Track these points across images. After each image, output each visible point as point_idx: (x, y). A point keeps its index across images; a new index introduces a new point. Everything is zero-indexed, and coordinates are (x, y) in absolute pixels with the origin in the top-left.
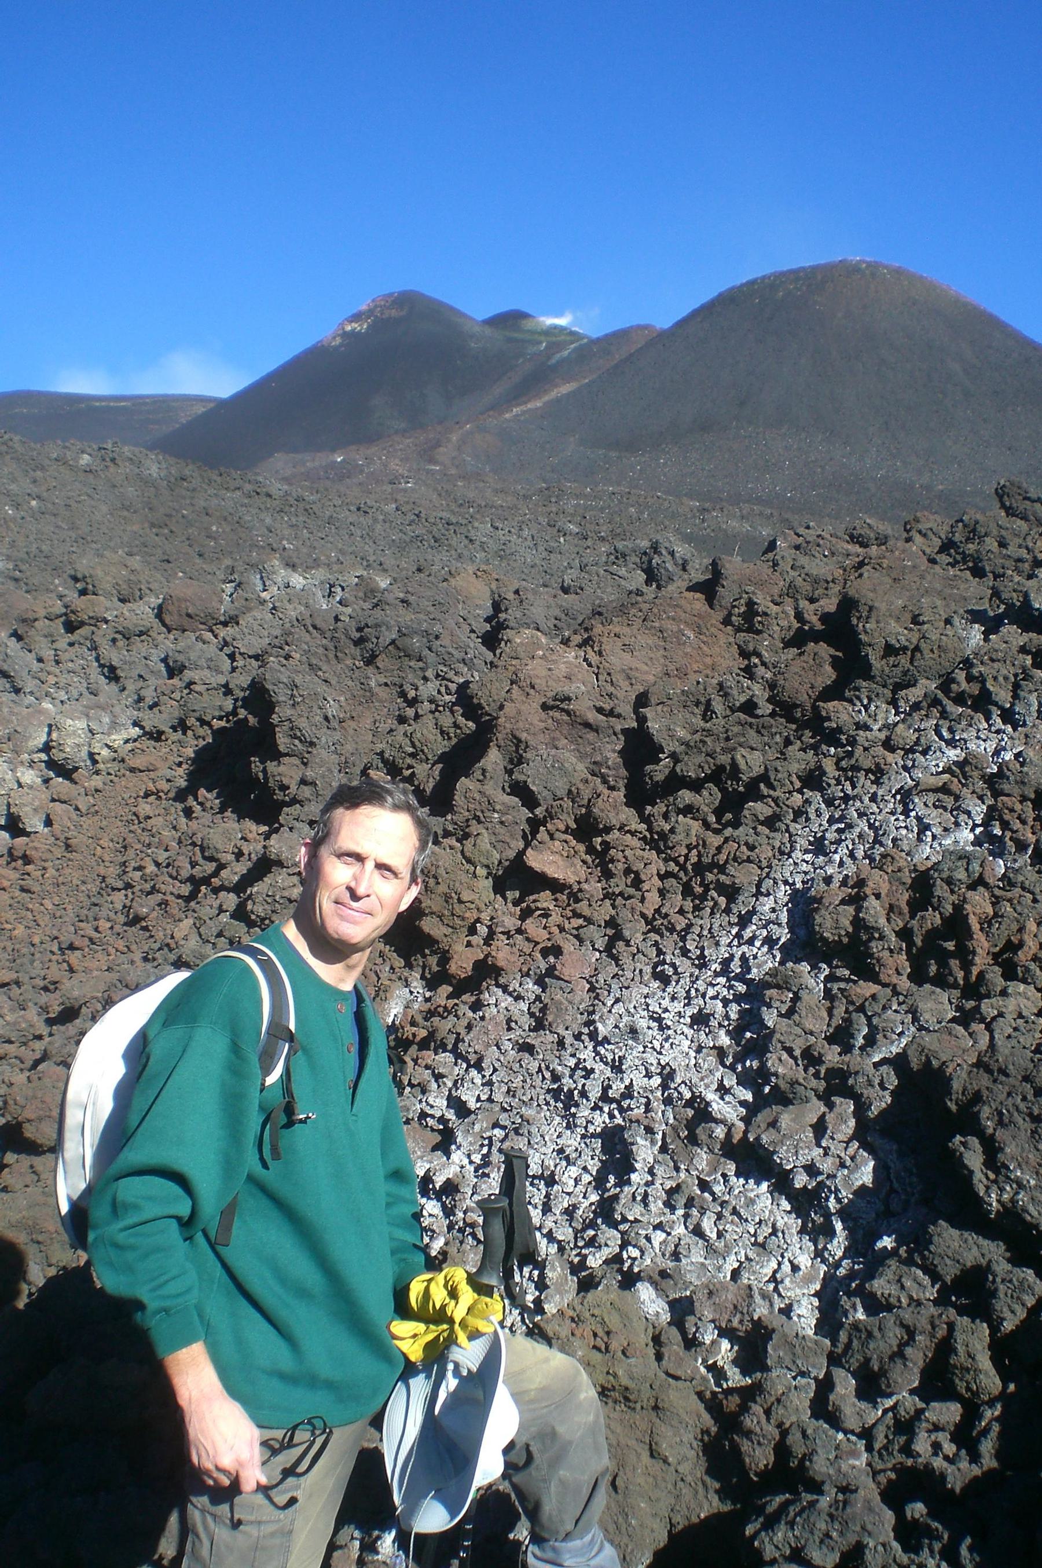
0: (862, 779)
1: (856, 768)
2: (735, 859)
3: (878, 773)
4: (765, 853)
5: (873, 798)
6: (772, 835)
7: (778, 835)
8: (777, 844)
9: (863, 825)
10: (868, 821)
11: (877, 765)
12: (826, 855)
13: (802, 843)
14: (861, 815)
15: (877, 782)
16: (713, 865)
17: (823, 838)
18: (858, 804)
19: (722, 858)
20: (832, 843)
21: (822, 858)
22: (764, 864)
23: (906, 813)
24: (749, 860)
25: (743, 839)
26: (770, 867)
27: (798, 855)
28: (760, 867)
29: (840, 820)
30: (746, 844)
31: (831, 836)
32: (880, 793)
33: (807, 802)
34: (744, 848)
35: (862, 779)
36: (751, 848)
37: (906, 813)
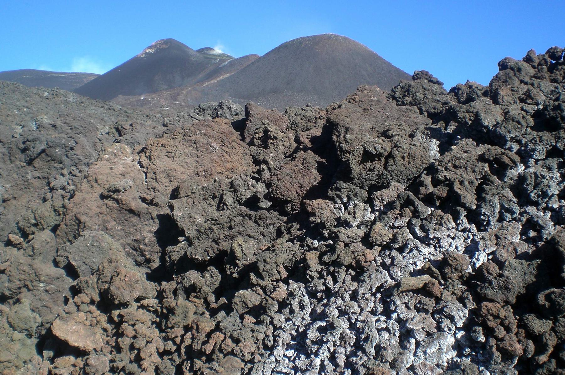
0: (343, 275)
1: (337, 264)
2: (221, 350)
3: (359, 271)
4: (249, 347)
5: (354, 296)
6: (256, 327)
7: (262, 328)
8: (261, 336)
9: (343, 325)
10: (349, 320)
11: (358, 262)
12: (308, 356)
13: (285, 337)
14: (342, 313)
15: (357, 278)
16: (200, 354)
17: (305, 333)
18: (340, 301)
19: (209, 348)
20: (314, 342)
21: (303, 357)
22: (248, 357)
23: (387, 313)
24: (232, 353)
25: (229, 329)
26: (252, 361)
27: (280, 351)
28: (243, 361)
29: (323, 316)
30: (231, 337)
31: (313, 334)
32: (361, 291)
33: (291, 294)
34: (229, 341)
35: (343, 275)
36: (237, 341)
37: (387, 313)
